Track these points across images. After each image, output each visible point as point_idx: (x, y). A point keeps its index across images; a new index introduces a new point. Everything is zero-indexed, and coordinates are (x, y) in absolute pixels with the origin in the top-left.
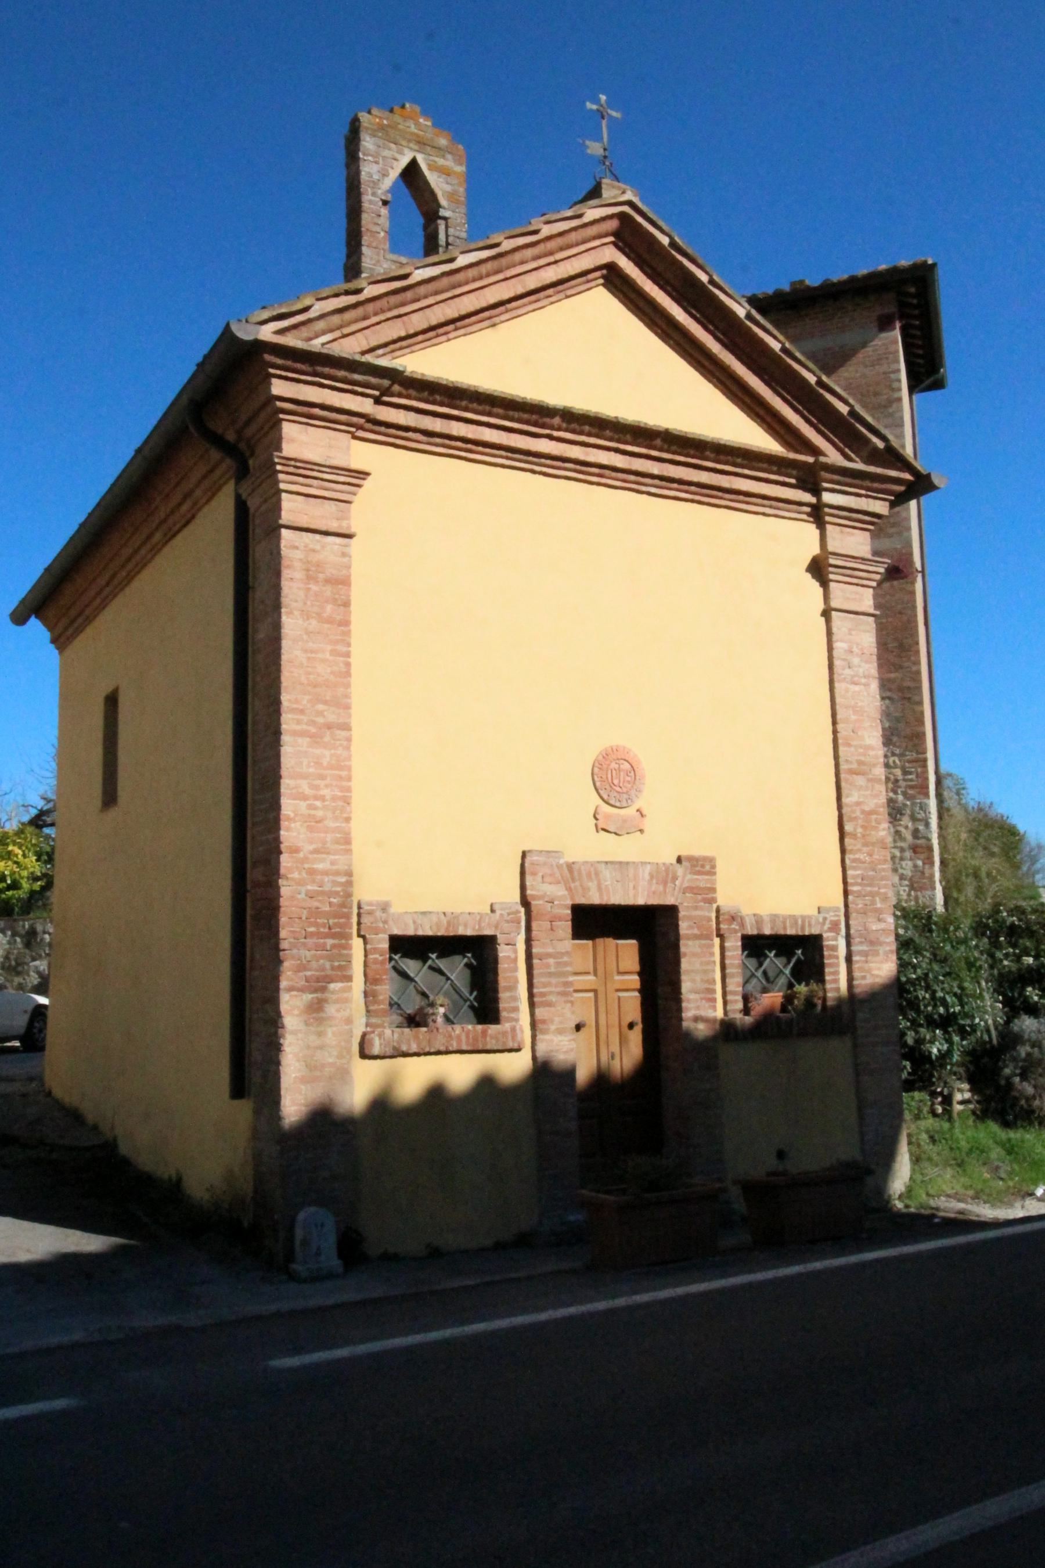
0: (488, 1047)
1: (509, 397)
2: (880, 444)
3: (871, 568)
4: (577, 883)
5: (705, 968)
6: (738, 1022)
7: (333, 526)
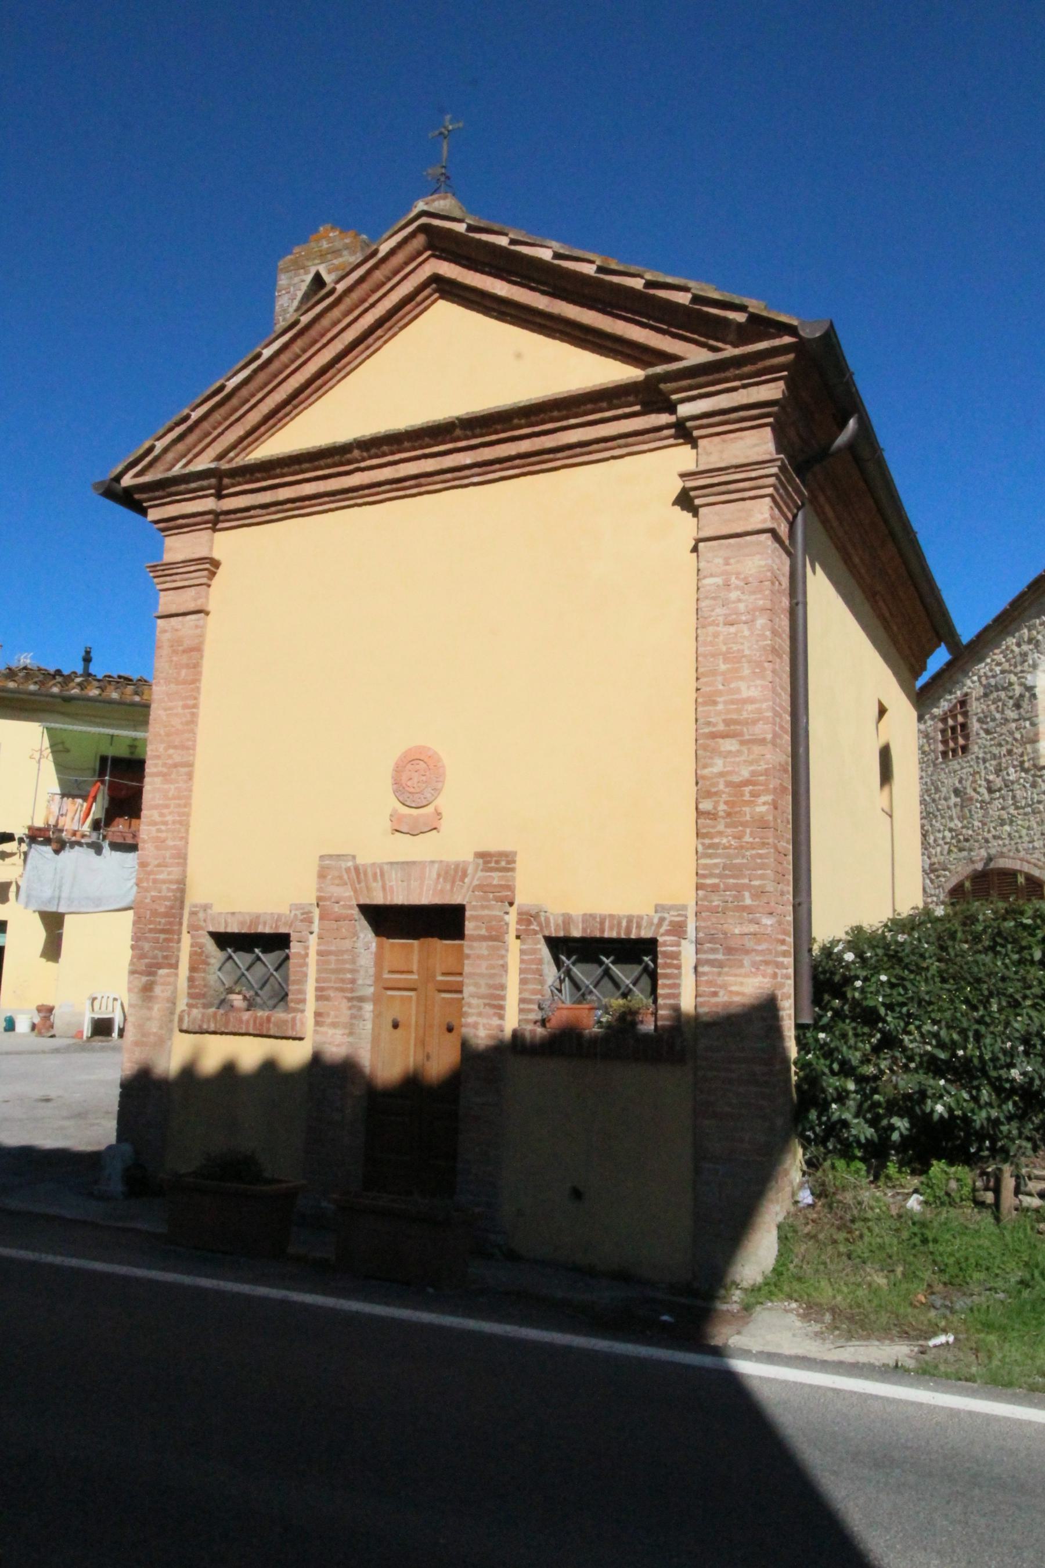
0: (272, 1033)
1: (305, 451)
2: (740, 317)
3: (753, 474)
4: (363, 884)
5: (493, 971)
6: (528, 1035)
7: (192, 606)
